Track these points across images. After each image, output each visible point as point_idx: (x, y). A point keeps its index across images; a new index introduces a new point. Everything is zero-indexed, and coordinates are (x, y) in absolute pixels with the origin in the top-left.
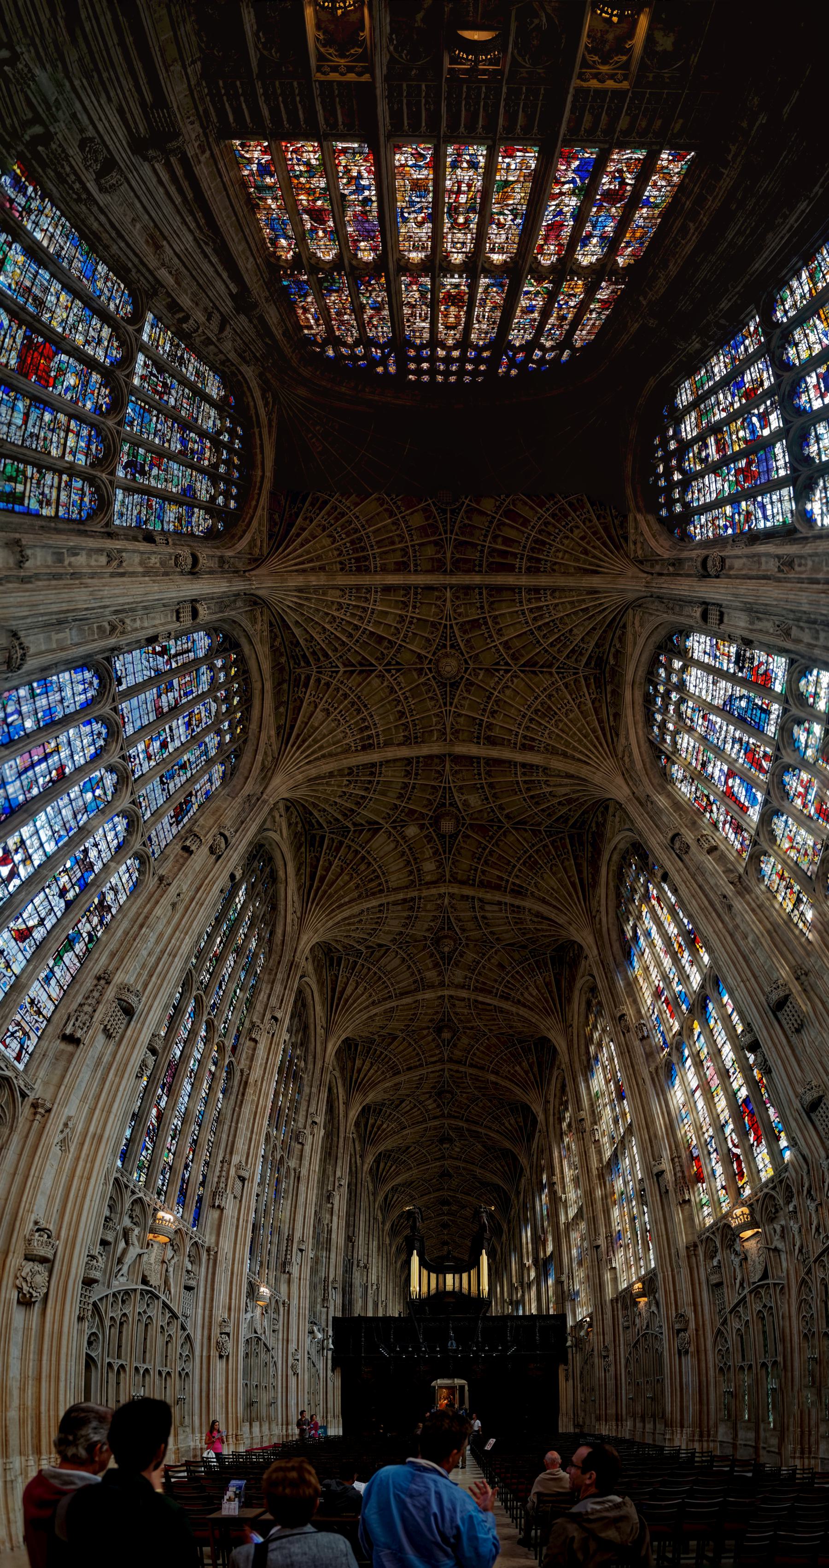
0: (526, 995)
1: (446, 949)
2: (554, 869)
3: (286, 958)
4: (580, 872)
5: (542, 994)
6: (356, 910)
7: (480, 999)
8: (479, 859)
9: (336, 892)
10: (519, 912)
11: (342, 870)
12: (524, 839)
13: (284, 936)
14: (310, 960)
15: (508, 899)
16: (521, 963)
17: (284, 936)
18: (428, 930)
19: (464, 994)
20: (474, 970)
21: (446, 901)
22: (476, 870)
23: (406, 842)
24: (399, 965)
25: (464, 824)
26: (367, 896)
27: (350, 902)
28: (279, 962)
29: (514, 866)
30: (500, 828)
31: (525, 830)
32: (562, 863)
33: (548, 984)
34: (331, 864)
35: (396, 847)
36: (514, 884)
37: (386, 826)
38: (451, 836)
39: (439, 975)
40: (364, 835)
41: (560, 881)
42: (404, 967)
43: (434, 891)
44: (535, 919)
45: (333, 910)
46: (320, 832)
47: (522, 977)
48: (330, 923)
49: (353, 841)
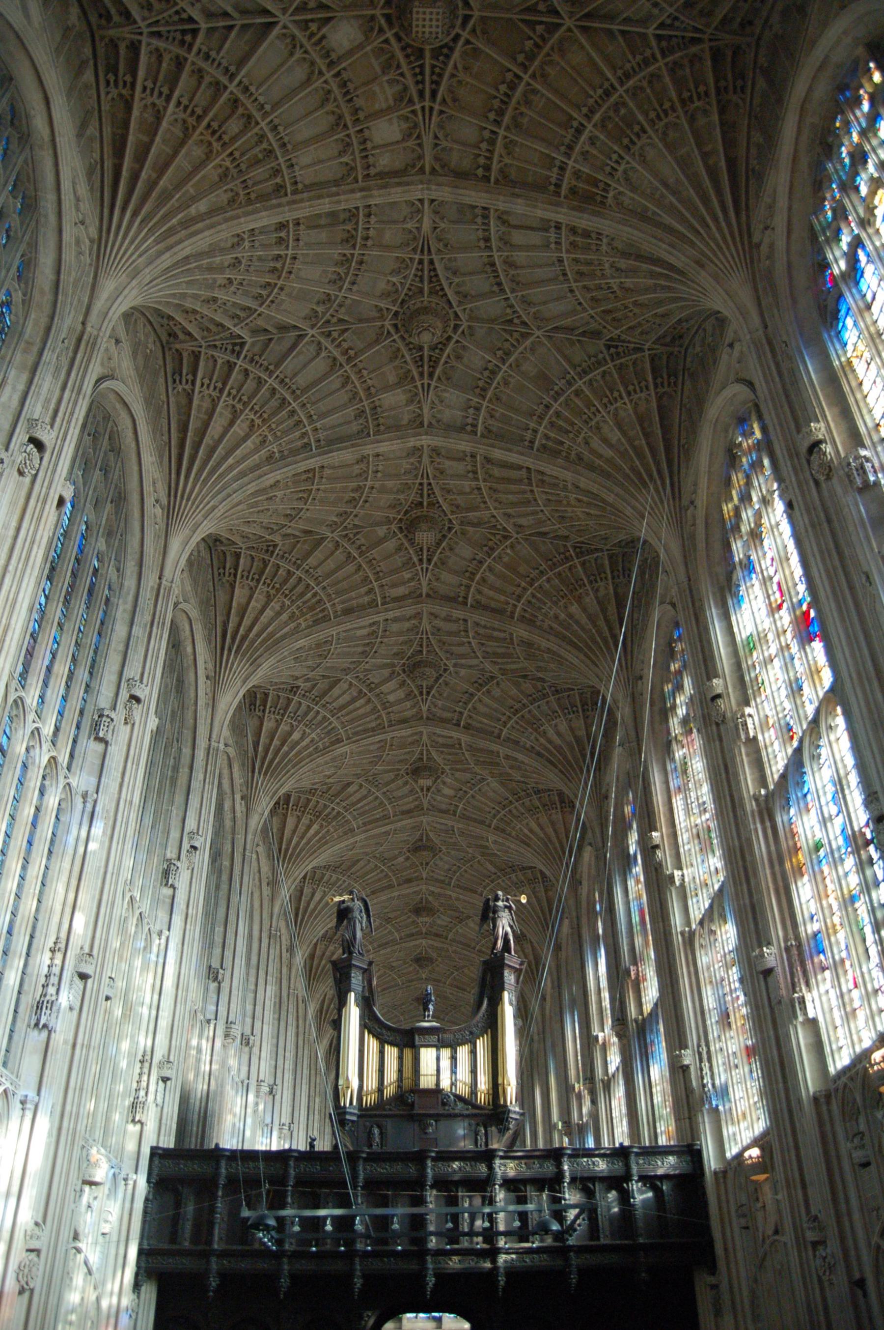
0: (596, 443)
1: (426, 339)
2: (672, 135)
3: (68, 321)
4: (729, 143)
5: (630, 441)
6: (224, 233)
7: (497, 454)
8: (501, 113)
9: (178, 187)
10: (587, 249)
11: (187, 132)
12: (607, 59)
13: (58, 272)
14: (126, 345)
15: (563, 215)
16: (585, 372)
17: (58, 272)
18: (385, 295)
19: (463, 445)
20: (484, 389)
21: (426, 225)
22: (492, 142)
23: (331, 64)
24: (325, 376)
25: (466, 19)
26: (249, 202)
27: (211, 213)
28: (48, 329)
29: (579, 131)
30: (553, 28)
31: (610, 32)
32: (692, 120)
33: (641, 420)
34: (158, 117)
35: (308, 81)
36: (577, 174)
37: (284, 19)
38: (437, 53)
39: (410, 402)
40: (233, 44)
41: (684, 164)
42: (335, 381)
43: (397, 194)
44: (623, 264)
45: (171, 232)
46: (125, 33)
47: (589, 404)
48: (167, 260)
49: (207, 57)
